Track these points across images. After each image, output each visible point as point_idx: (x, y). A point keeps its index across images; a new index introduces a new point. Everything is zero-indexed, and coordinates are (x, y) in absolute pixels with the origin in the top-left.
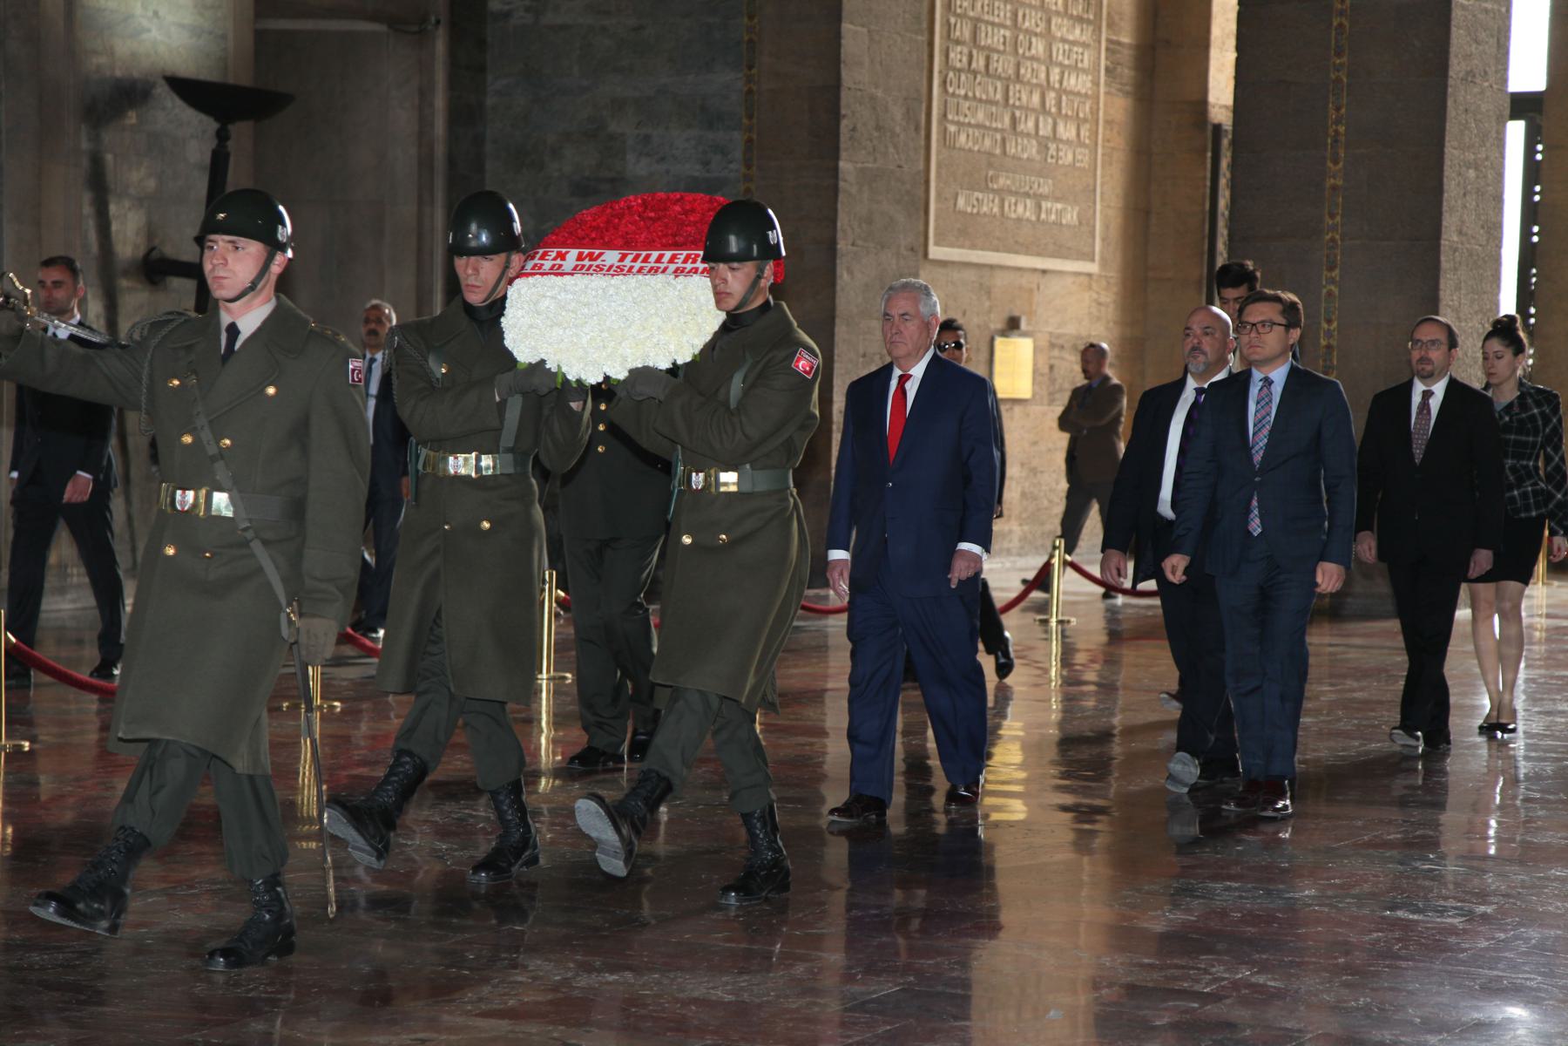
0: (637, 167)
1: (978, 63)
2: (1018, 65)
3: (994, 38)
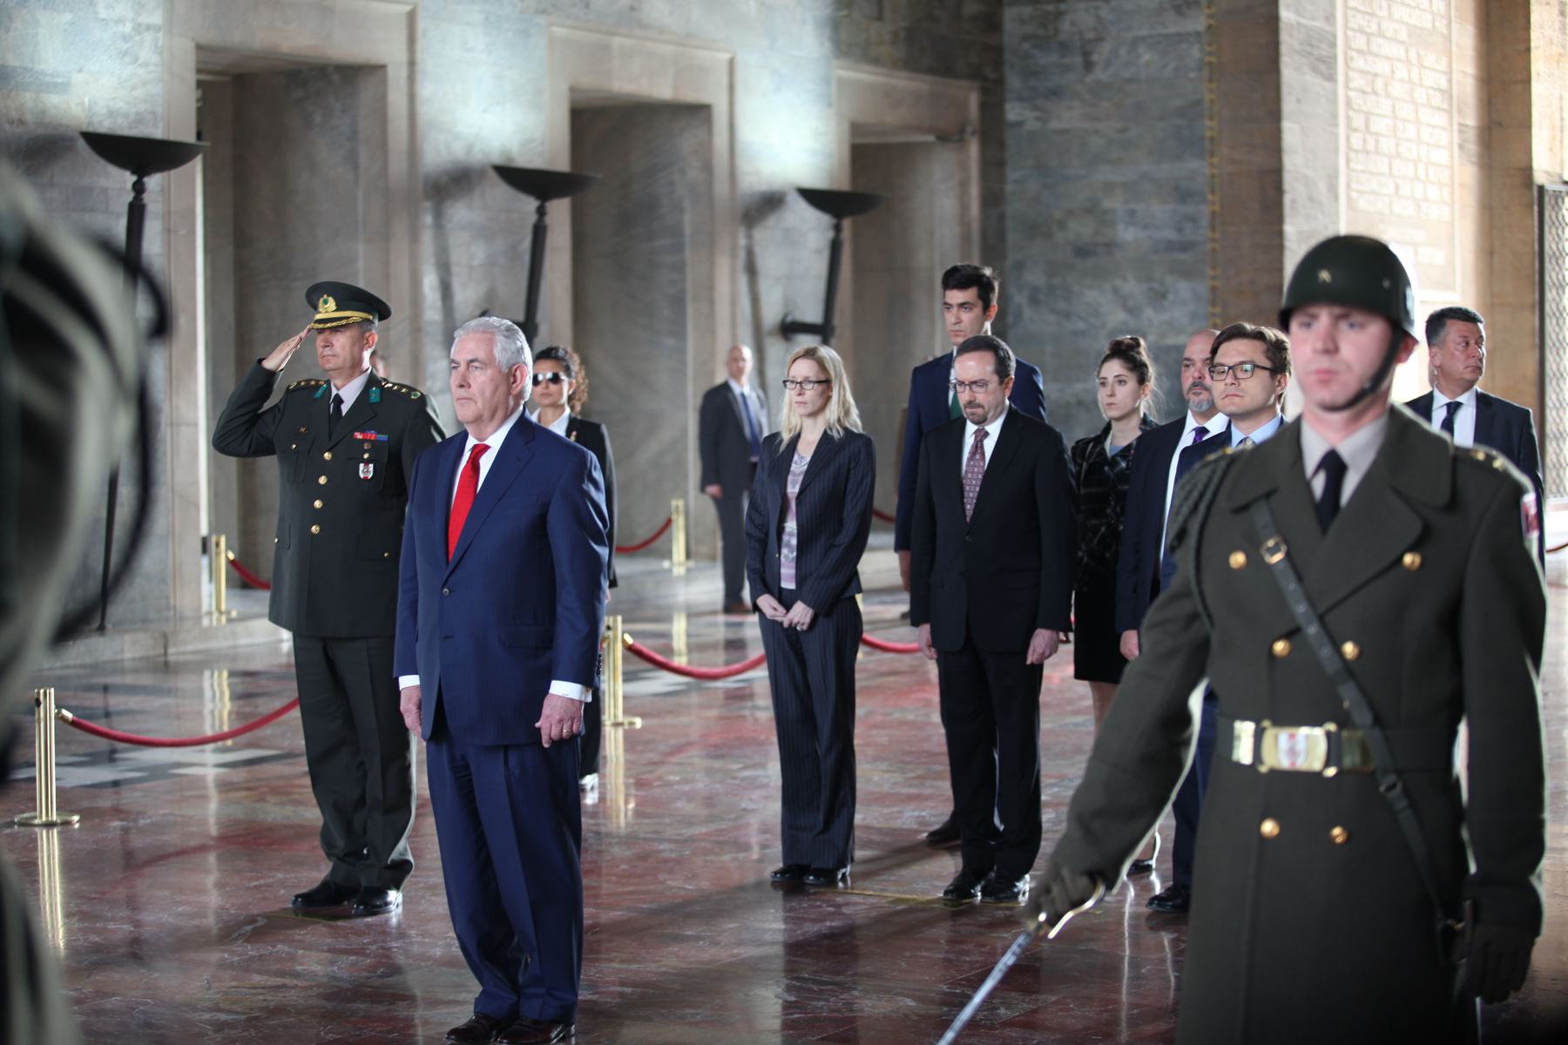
0: (1127, 234)
1: (1371, 145)
2: (1397, 146)
3: (1380, 125)
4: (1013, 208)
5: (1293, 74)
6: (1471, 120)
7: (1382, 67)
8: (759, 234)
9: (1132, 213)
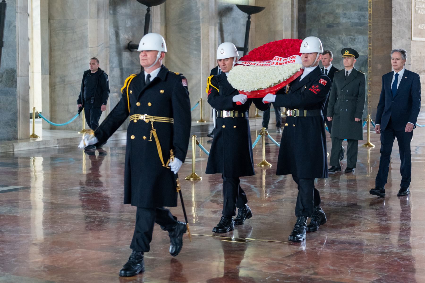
0: (343, 20)
4: (309, 12)
8: (224, 19)
9: (345, 14)
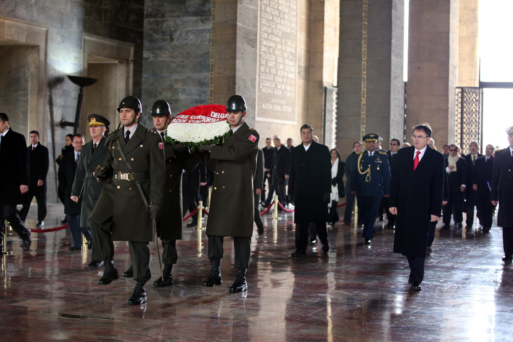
0: (182, 97)
1: (268, 70)
2: (277, 71)
3: (271, 64)
4: (144, 87)
5: (241, 45)
6: (303, 64)
7: (272, 44)
9: (184, 90)
